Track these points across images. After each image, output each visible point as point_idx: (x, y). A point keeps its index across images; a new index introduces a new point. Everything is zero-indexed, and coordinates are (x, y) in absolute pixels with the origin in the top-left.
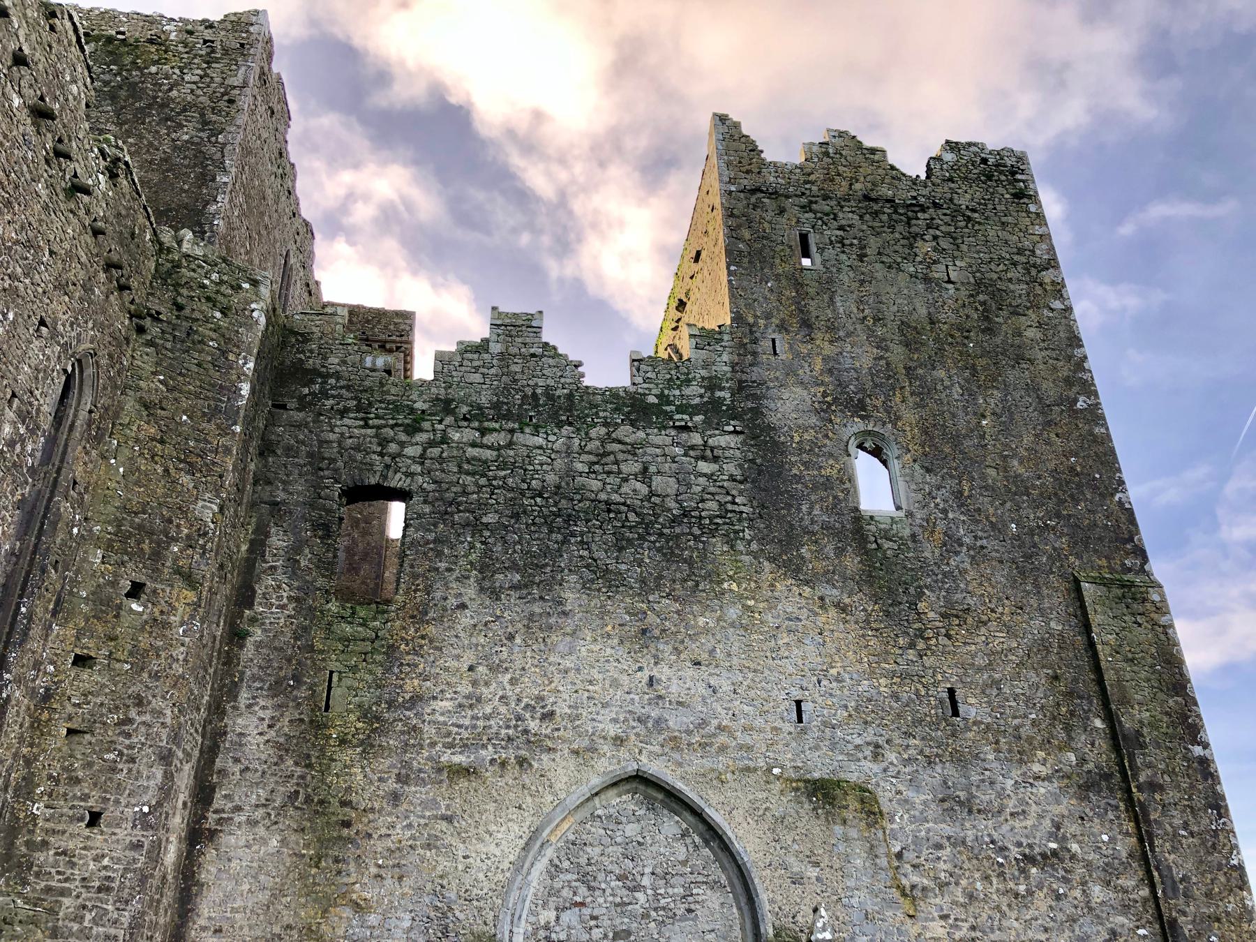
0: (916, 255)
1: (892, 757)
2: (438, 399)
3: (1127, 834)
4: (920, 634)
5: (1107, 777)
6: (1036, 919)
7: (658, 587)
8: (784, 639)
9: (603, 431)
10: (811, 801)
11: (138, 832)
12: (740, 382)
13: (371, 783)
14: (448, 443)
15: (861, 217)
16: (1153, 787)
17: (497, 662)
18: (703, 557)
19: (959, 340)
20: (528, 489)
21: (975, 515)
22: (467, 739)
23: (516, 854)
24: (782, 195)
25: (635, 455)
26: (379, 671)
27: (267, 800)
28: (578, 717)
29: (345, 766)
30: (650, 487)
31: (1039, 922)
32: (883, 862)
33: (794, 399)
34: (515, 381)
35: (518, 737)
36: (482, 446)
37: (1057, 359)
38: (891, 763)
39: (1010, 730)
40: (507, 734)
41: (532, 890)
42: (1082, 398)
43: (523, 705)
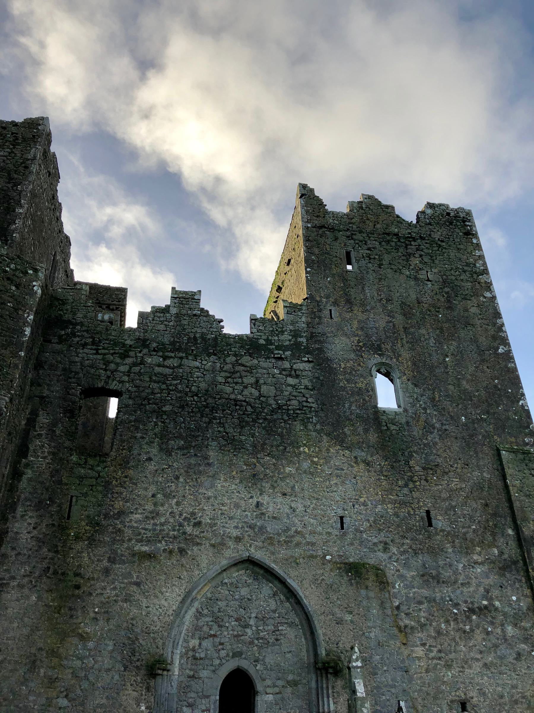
0: (410, 265)
1: (394, 550)
2: (139, 339)
3: (526, 596)
4: (411, 479)
5: (515, 563)
6: (475, 646)
7: (263, 450)
8: (334, 481)
9: (234, 359)
10: (348, 575)
12: (312, 333)
13: (93, 562)
14: (144, 364)
15: (380, 243)
17: (169, 492)
18: (289, 431)
19: (433, 313)
20: (190, 391)
21: (442, 411)
22: (150, 537)
23: (177, 605)
24: (336, 230)
25: (251, 373)
26: (100, 496)
27: (31, 573)
28: (215, 524)
29: (78, 552)
30: (260, 391)
31: (477, 647)
32: (389, 612)
33: (342, 343)
34: (184, 329)
35: (180, 536)
36: (164, 366)
37: (488, 325)
38: (394, 553)
39: (461, 535)
40: (173, 534)
41: (185, 627)
42: (501, 347)
43: (183, 517)
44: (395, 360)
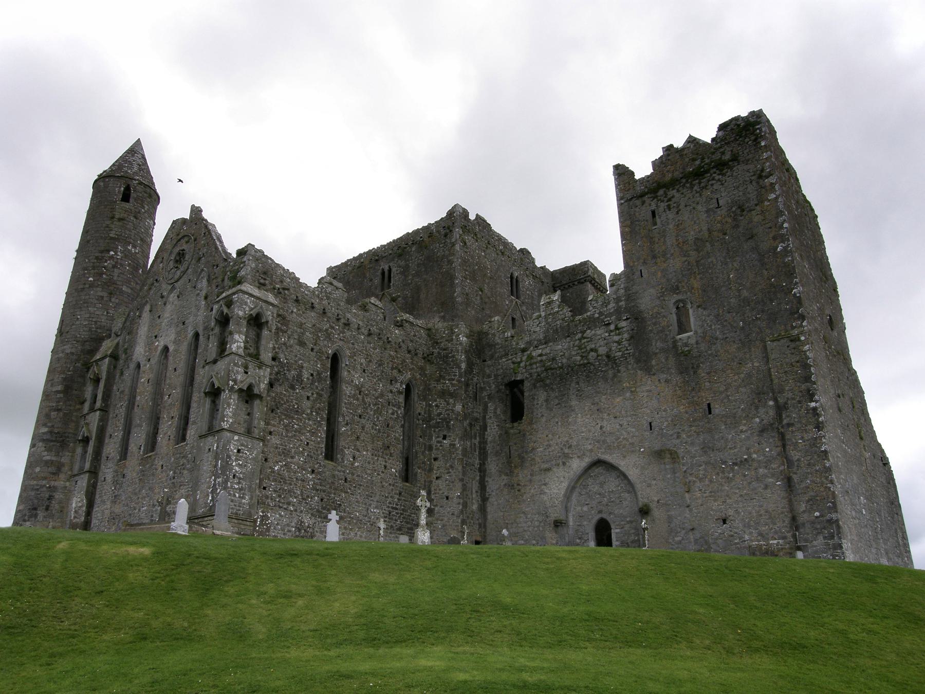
3: (777, 447)
5: (772, 425)
11: (458, 499)
16: (789, 425)
44: (689, 293)
